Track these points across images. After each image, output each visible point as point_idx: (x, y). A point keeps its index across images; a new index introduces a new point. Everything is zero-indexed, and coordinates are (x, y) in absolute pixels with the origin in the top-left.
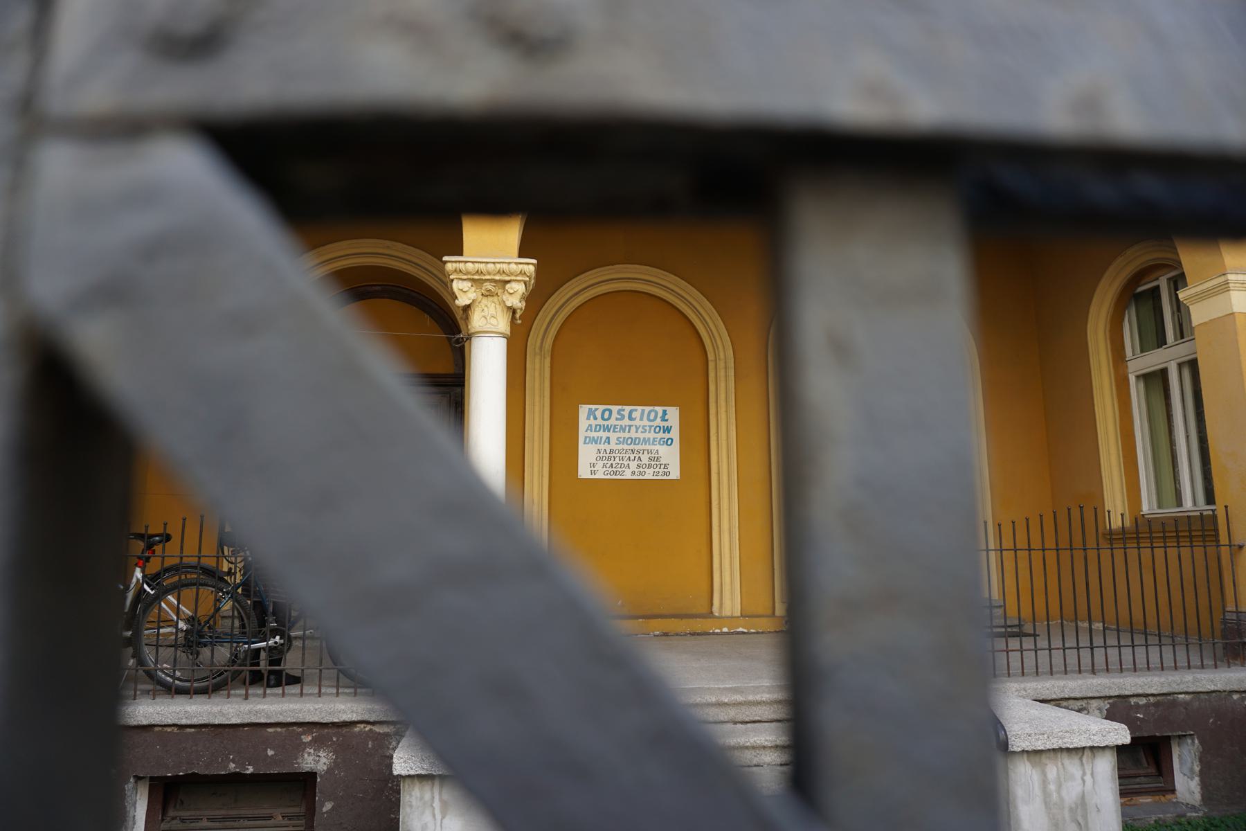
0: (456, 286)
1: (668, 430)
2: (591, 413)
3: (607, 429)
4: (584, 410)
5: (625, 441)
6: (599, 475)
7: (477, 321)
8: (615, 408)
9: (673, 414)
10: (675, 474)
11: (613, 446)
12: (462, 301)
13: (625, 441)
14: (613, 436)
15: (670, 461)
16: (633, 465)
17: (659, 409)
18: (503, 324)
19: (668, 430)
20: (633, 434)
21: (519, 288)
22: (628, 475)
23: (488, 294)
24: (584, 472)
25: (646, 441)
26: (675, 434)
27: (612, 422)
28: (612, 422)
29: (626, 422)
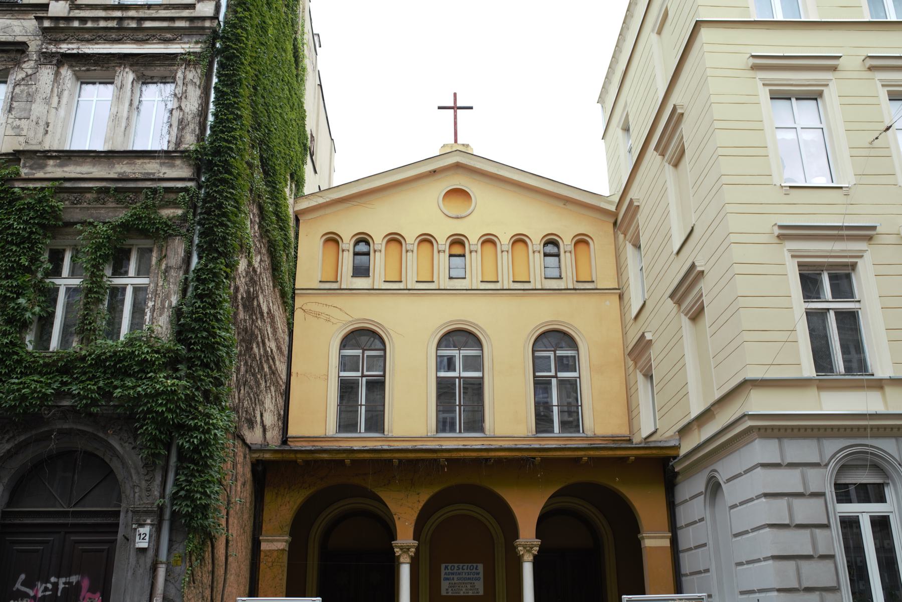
0: (396, 550)
1: (478, 574)
2: (446, 567)
3: (453, 574)
4: (443, 566)
5: (460, 579)
6: (450, 594)
7: (402, 560)
8: (456, 565)
9: (480, 567)
10: (481, 593)
11: (455, 581)
12: (397, 554)
13: (460, 579)
14: (456, 577)
15: (479, 588)
16: (464, 589)
17: (475, 565)
18: (408, 560)
19: (478, 574)
20: (464, 576)
21: (413, 550)
22: (462, 594)
23: (404, 552)
24: (444, 593)
25: (469, 579)
26: (481, 575)
27: (455, 571)
28: (455, 571)
29: (461, 571)
